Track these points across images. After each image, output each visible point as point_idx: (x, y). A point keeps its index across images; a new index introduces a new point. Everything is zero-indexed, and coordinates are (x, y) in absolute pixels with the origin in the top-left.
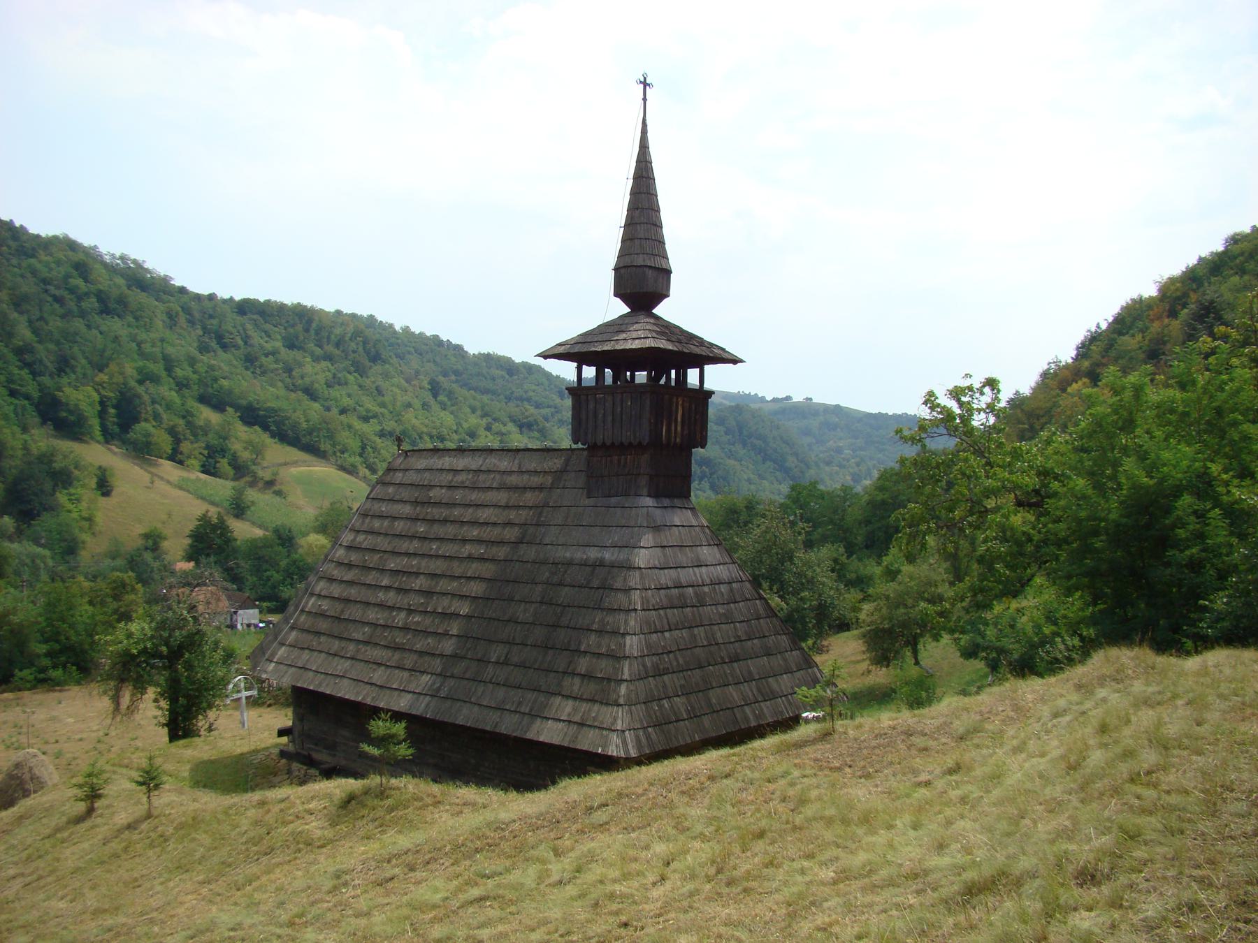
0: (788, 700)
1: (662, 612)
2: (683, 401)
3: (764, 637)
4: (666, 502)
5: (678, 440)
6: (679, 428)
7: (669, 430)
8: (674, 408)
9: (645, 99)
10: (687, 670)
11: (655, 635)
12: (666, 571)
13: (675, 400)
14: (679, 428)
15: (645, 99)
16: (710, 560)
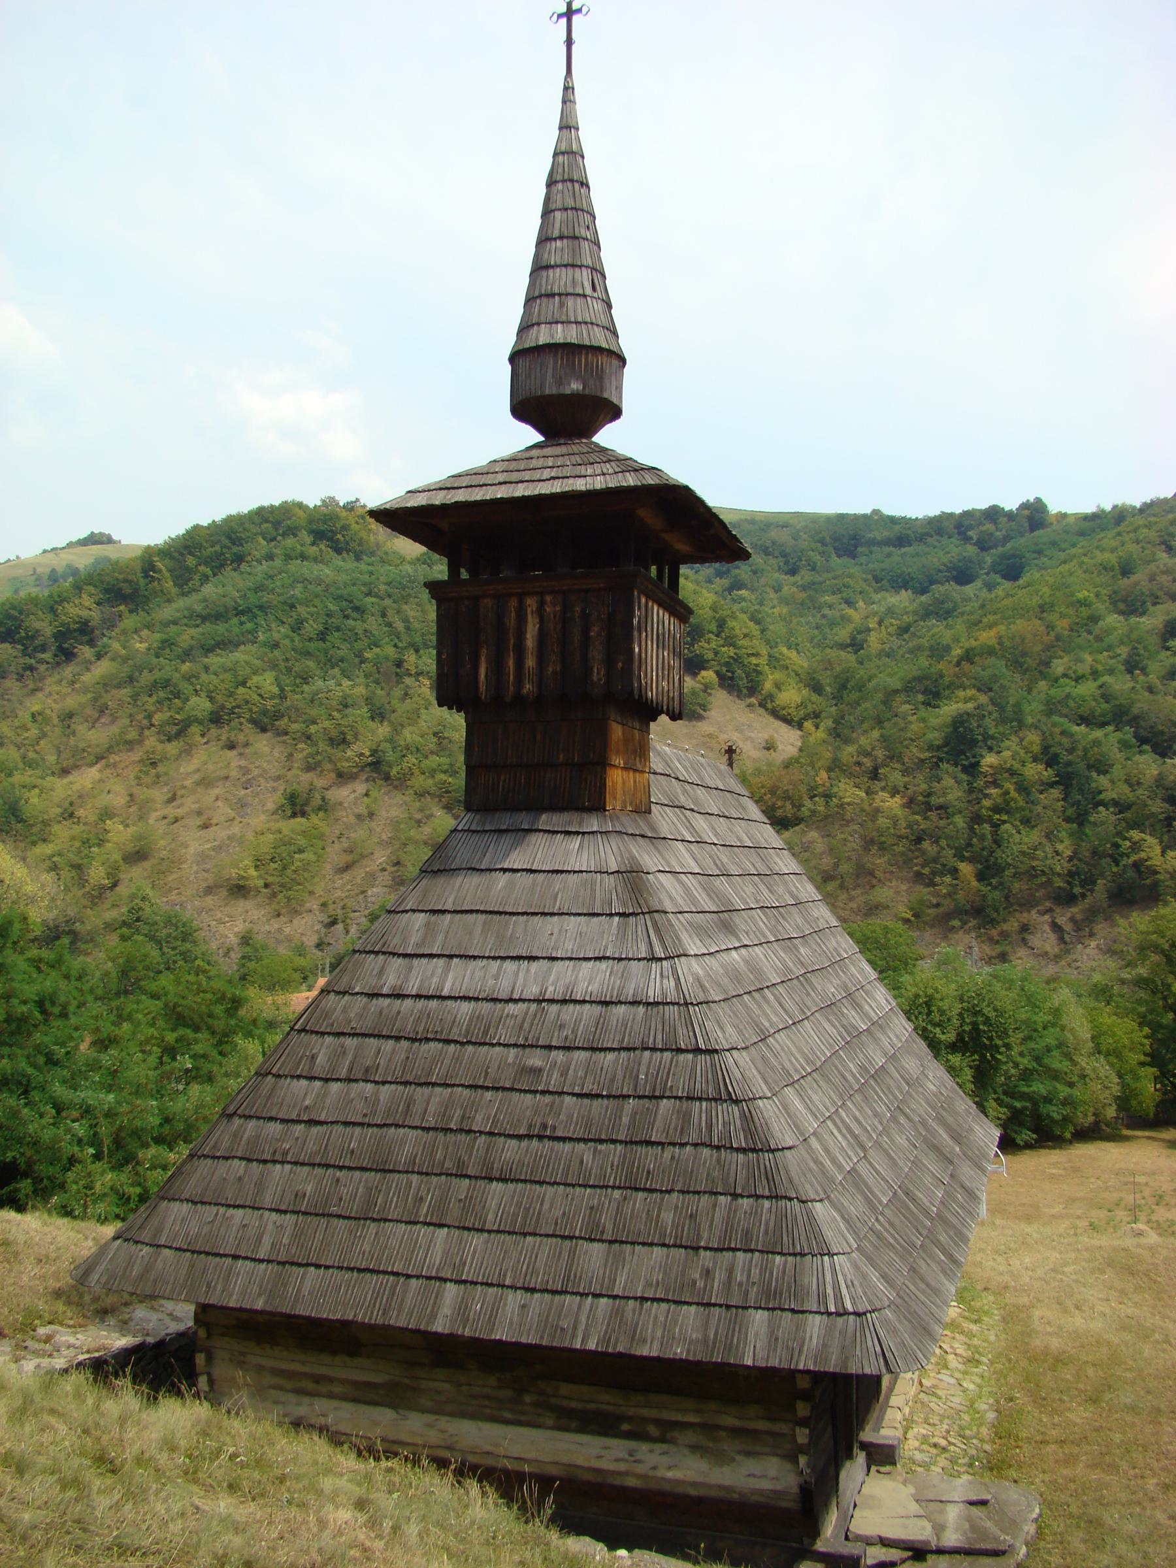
0: (617, 1313)
1: (350, 1042)
2: (542, 604)
3: (649, 1143)
4: (506, 820)
5: (528, 687)
6: (530, 662)
7: (497, 667)
8: (511, 620)
9: (569, 42)
10: (341, 1168)
11: (304, 1082)
12: (416, 962)
13: (513, 603)
14: (530, 662)
15: (569, 42)
16: (568, 947)
